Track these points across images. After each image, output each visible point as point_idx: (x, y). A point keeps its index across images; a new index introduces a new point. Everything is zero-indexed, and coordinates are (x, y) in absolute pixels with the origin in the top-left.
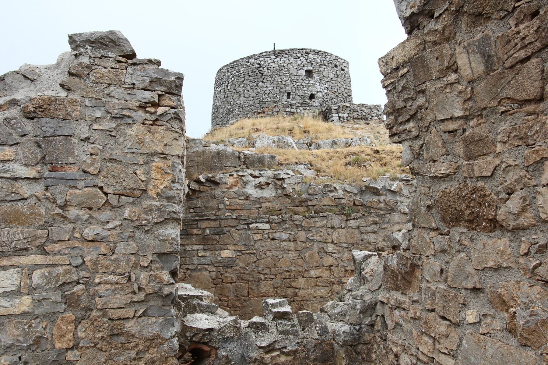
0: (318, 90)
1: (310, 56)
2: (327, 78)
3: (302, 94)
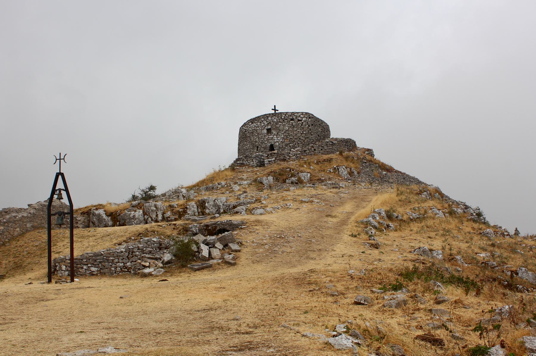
0: (276, 141)
1: (270, 118)
2: (283, 131)
3: (265, 146)
